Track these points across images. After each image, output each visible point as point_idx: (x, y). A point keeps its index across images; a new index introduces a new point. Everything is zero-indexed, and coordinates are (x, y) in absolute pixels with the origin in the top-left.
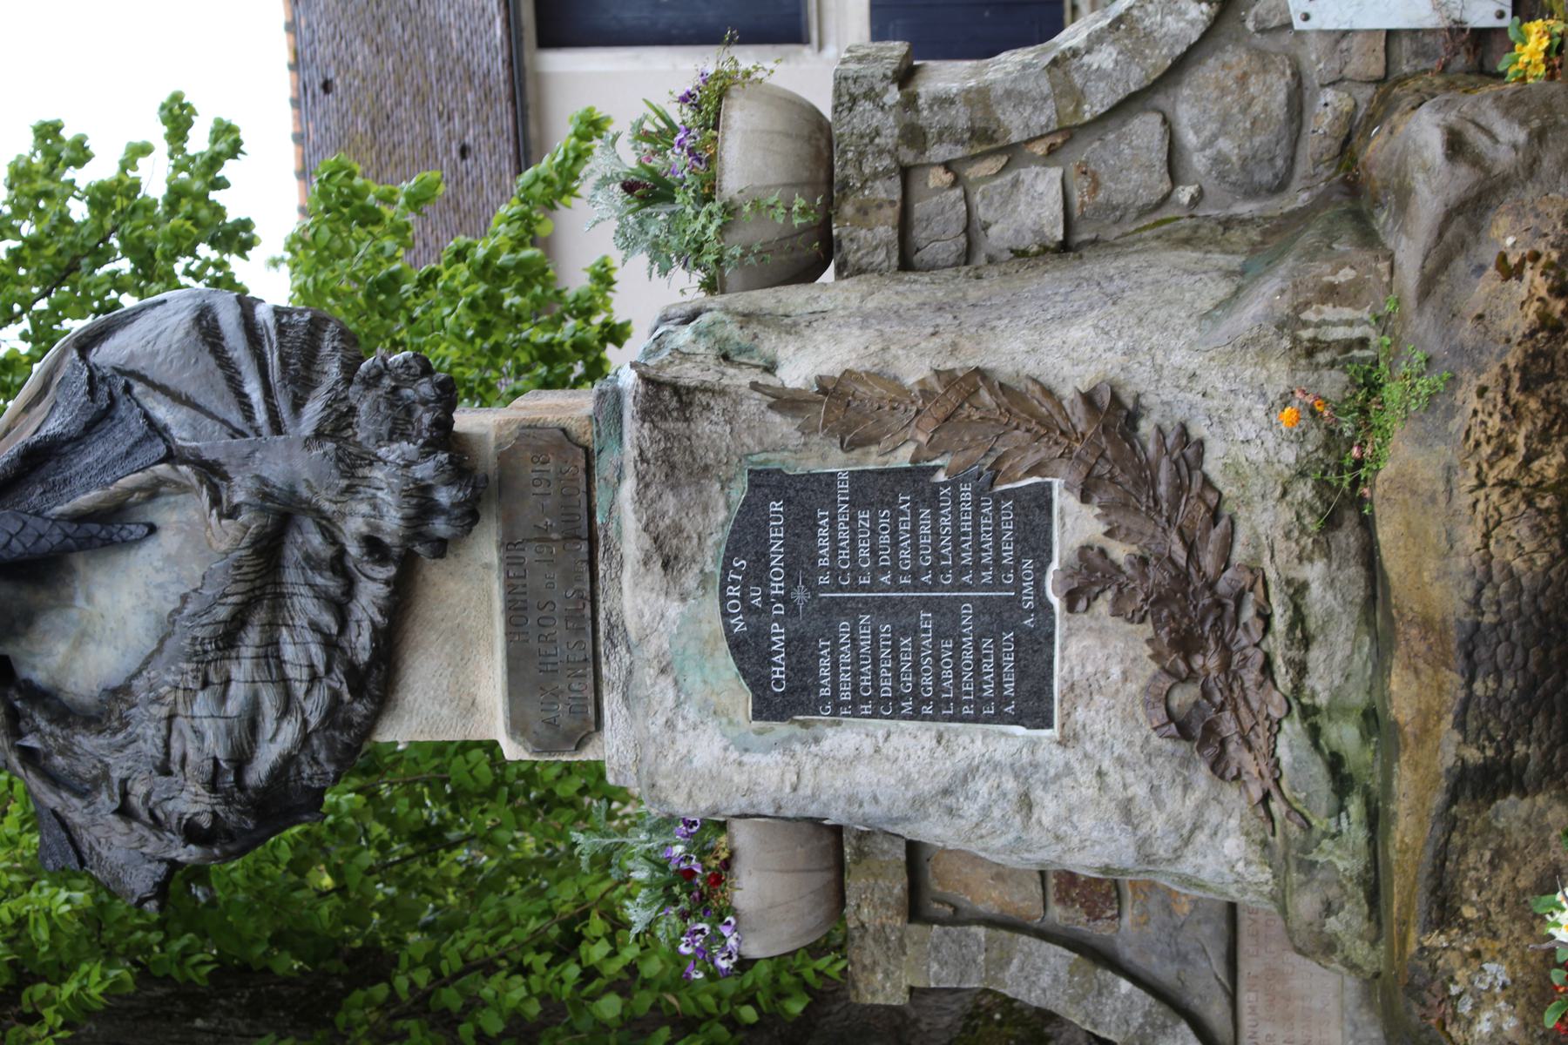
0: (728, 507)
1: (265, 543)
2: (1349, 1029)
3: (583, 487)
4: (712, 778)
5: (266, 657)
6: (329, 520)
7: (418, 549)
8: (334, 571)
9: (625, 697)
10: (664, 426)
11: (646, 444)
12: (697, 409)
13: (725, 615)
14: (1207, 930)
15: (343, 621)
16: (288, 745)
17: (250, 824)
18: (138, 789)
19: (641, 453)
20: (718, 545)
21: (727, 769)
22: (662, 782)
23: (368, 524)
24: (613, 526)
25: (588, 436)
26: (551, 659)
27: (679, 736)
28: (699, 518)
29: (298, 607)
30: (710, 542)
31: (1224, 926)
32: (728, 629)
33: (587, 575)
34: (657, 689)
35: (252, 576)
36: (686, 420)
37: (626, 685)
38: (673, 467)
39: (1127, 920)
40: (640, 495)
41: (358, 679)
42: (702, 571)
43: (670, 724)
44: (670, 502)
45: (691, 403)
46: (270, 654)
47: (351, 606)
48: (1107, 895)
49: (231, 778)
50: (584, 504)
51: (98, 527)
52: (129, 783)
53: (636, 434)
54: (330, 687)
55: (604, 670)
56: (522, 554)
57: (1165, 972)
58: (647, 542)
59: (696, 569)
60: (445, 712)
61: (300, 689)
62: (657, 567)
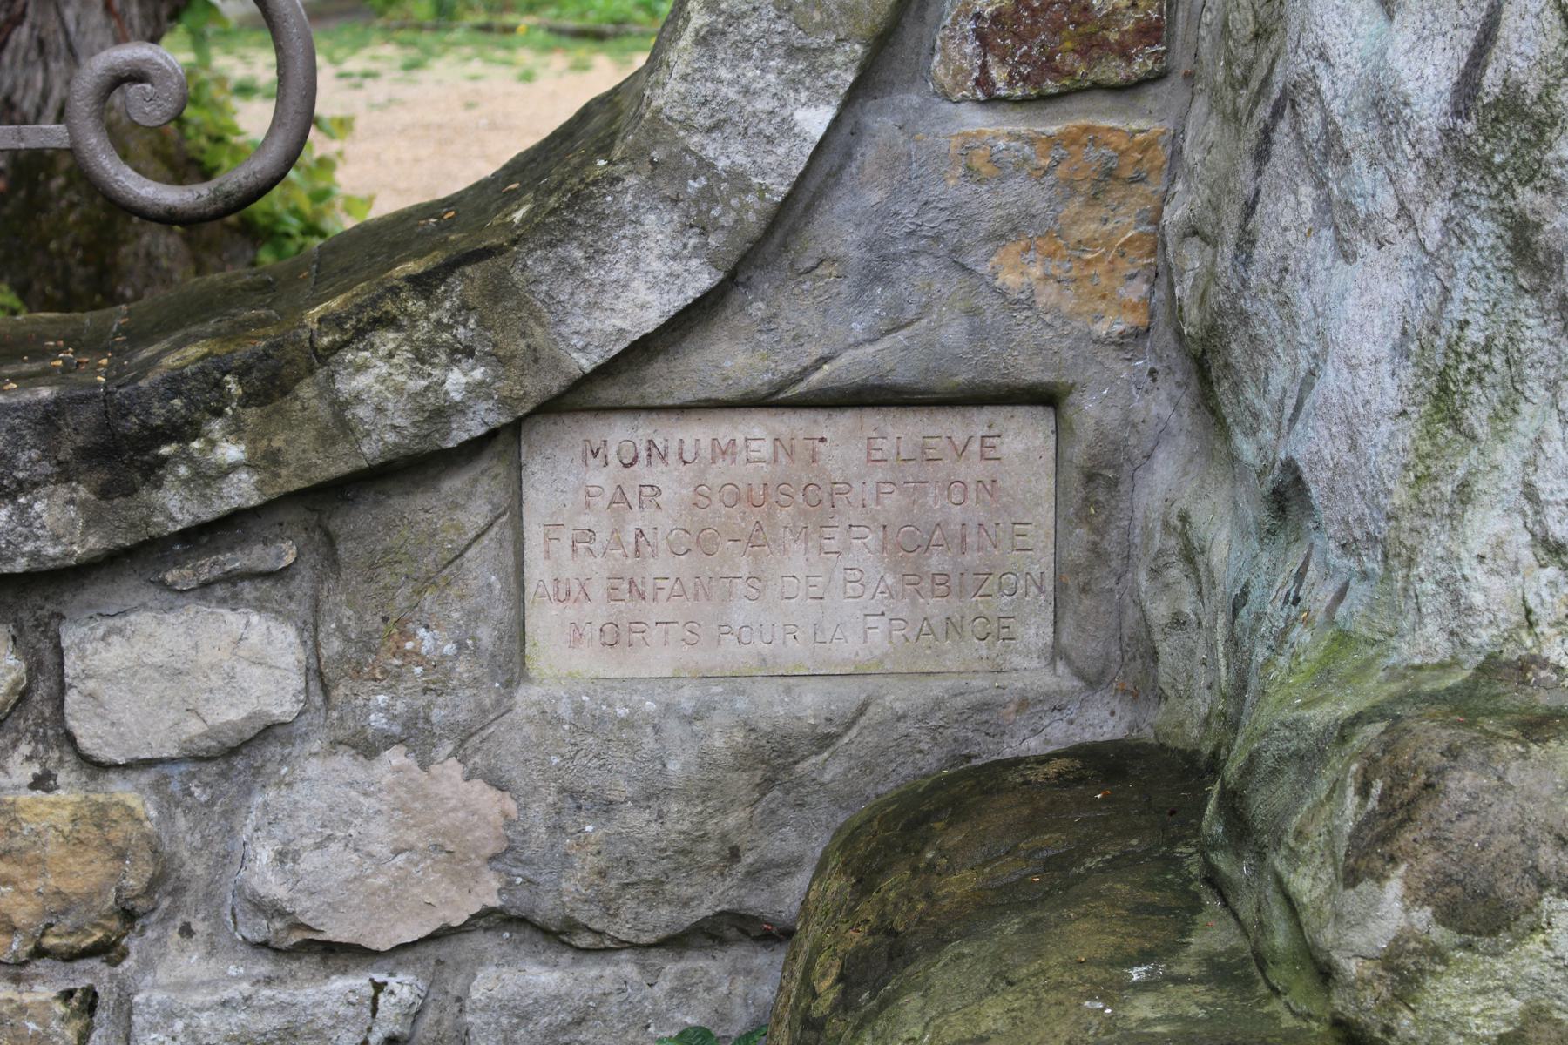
2: (686, 698)
14: (954, 334)
31: (963, 377)
39: (977, 120)
48: (1048, 66)
57: (839, 230)
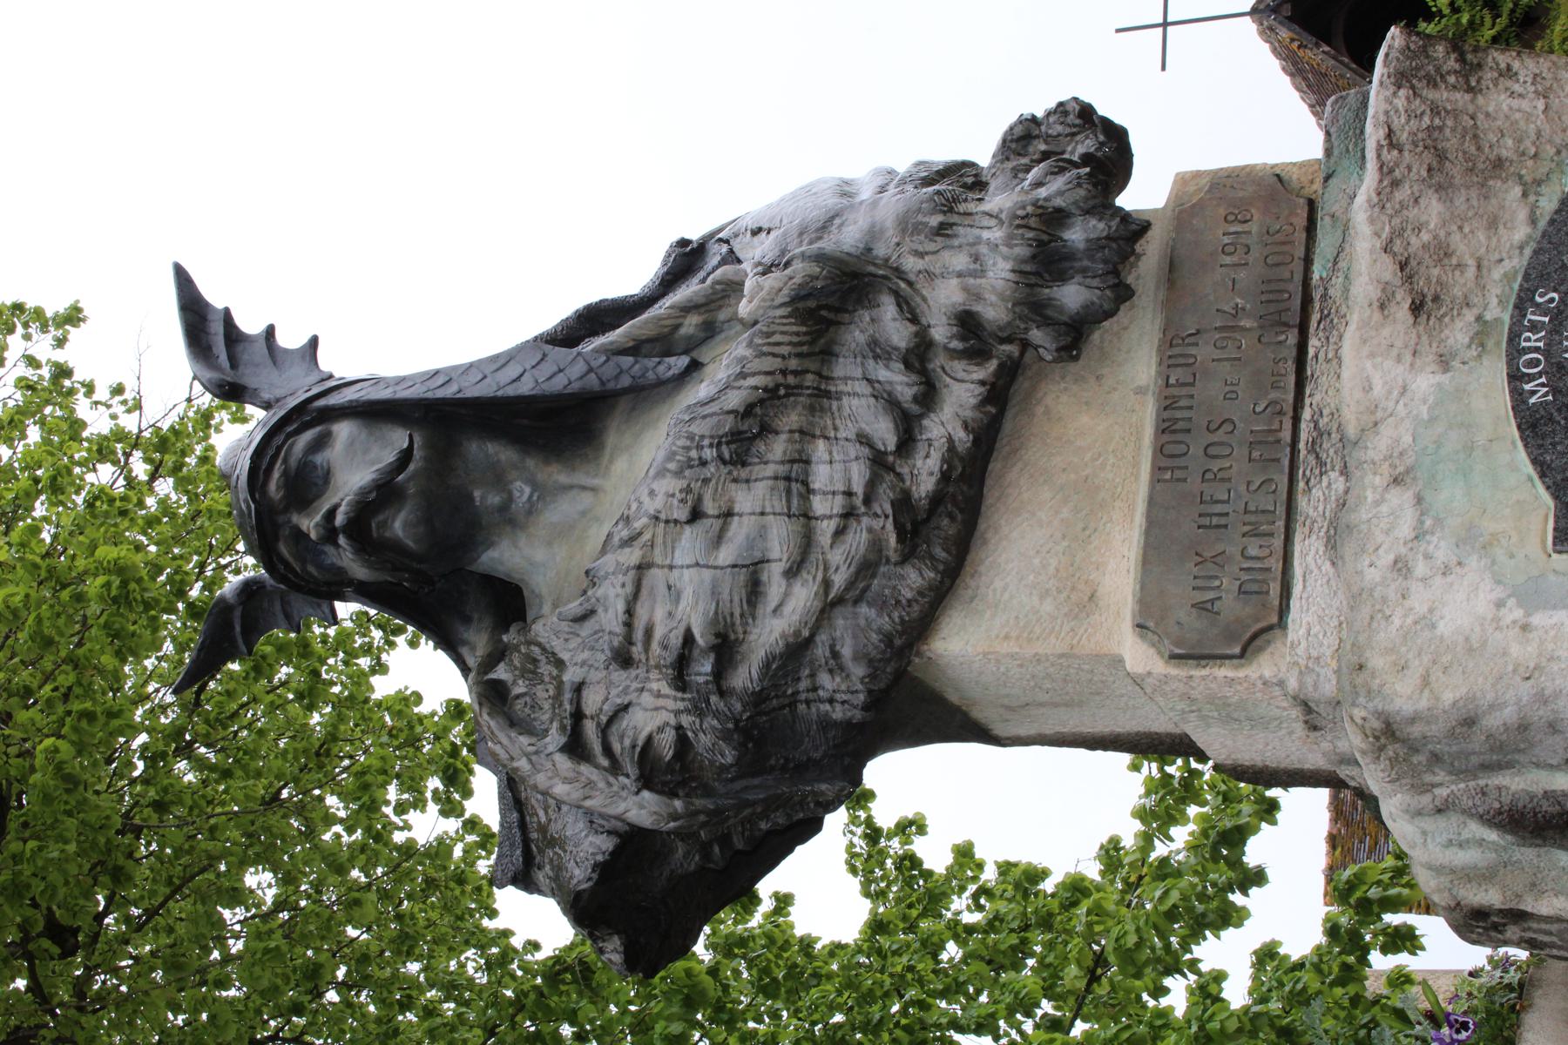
0: (1533, 221)
1: (812, 304)
3: (1300, 252)
4: (1470, 650)
5: (788, 479)
6: (910, 284)
7: (1036, 335)
8: (908, 366)
9: (1332, 544)
10: (1431, 94)
11: (1398, 122)
12: (1489, 75)
13: (1515, 377)
15: (907, 442)
16: (796, 617)
17: (729, 756)
18: (593, 701)
19: (1390, 134)
20: (1508, 277)
21: (1499, 635)
22: (1377, 661)
23: (966, 289)
24: (1338, 281)
25: (1315, 187)
26: (1218, 508)
27: (1415, 587)
28: (1481, 236)
29: (847, 411)
30: (1497, 274)
32: (1519, 398)
33: (1292, 379)
34: (1384, 509)
35: (785, 350)
36: (1470, 90)
37: (1334, 524)
38: (1441, 156)
40: (1381, 200)
41: (913, 524)
42: (1479, 318)
43: (1401, 567)
44: (1432, 210)
45: (1479, 66)
46: (796, 481)
47: (925, 422)
49: (707, 667)
50: (1298, 277)
51: (631, 359)
52: (585, 693)
53: (1384, 106)
54: (870, 530)
55: (1302, 502)
56: (1193, 351)
58: (1388, 269)
59: (1470, 316)
60: (1048, 607)
61: (826, 529)
62: (1402, 312)
